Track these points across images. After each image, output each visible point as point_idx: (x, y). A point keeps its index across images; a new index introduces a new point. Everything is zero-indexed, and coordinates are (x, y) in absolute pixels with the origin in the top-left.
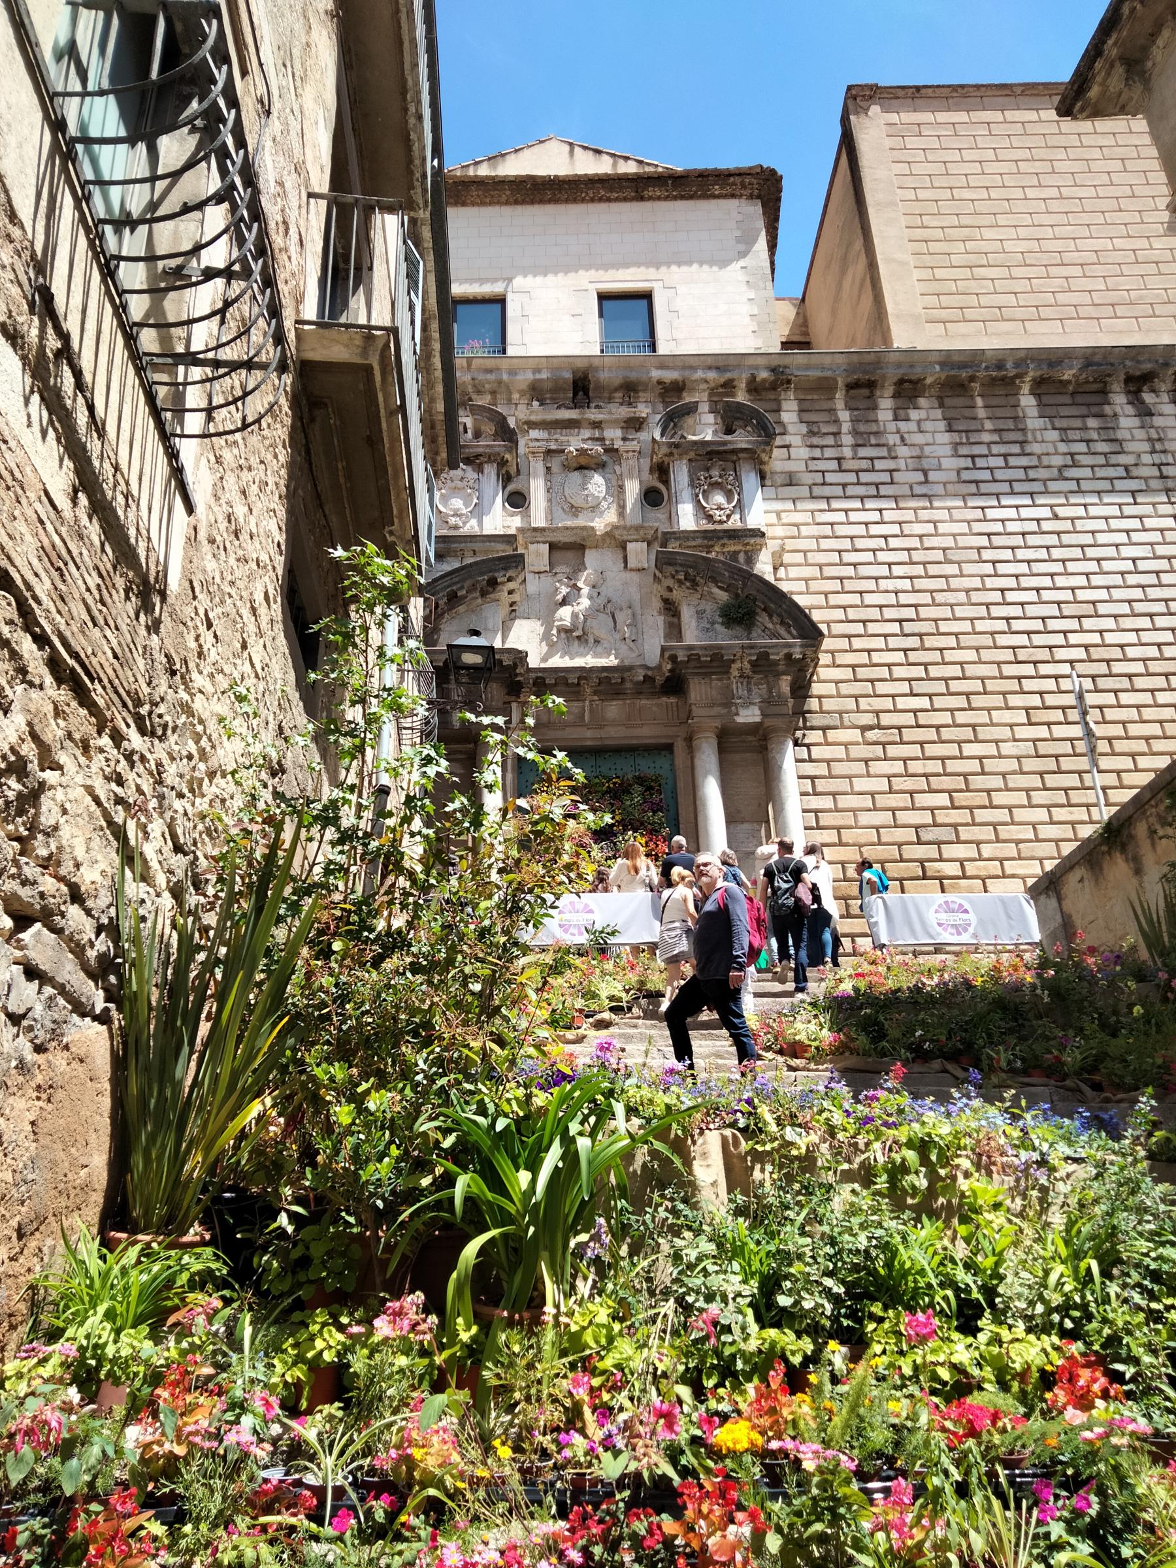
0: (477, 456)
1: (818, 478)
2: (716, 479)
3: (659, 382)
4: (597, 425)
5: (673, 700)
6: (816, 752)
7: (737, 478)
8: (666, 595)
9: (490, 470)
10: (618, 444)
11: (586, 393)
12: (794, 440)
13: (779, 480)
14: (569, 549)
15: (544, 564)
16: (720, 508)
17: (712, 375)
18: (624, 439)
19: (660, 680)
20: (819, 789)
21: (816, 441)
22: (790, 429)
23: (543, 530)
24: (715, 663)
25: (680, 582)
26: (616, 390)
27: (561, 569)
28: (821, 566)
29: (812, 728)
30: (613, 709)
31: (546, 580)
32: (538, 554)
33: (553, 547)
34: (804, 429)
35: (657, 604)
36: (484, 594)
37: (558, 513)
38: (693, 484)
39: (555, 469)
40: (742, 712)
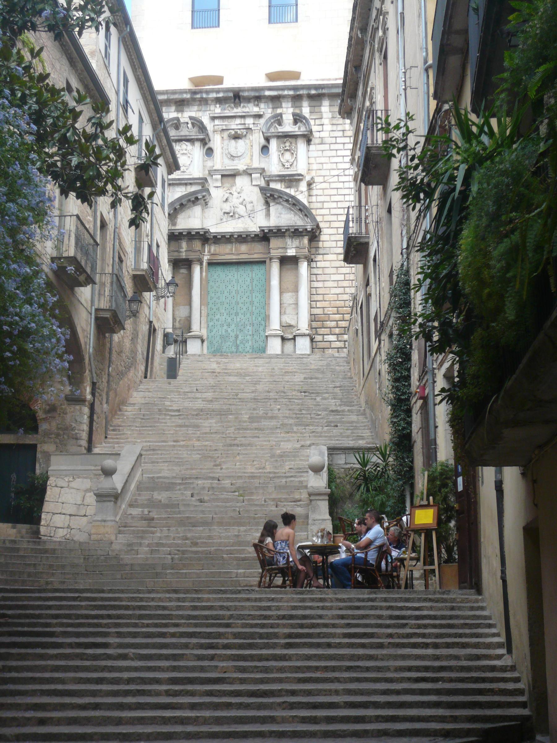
0: (192, 139)
1: (333, 140)
2: (288, 148)
4: (243, 117)
7: (296, 147)
9: (198, 144)
12: (326, 121)
14: (230, 176)
15: (219, 184)
16: (288, 161)
21: (335, 122)
22: (325, 115)
24: (279, 233)
27: (227, 185)
30: (244, 248)
31: (220, 190)
32: (216, 180)
33: (223, 176)
34: (330, 115)
35: (262, 201)
37: (227, 161)
40: (289, 251)
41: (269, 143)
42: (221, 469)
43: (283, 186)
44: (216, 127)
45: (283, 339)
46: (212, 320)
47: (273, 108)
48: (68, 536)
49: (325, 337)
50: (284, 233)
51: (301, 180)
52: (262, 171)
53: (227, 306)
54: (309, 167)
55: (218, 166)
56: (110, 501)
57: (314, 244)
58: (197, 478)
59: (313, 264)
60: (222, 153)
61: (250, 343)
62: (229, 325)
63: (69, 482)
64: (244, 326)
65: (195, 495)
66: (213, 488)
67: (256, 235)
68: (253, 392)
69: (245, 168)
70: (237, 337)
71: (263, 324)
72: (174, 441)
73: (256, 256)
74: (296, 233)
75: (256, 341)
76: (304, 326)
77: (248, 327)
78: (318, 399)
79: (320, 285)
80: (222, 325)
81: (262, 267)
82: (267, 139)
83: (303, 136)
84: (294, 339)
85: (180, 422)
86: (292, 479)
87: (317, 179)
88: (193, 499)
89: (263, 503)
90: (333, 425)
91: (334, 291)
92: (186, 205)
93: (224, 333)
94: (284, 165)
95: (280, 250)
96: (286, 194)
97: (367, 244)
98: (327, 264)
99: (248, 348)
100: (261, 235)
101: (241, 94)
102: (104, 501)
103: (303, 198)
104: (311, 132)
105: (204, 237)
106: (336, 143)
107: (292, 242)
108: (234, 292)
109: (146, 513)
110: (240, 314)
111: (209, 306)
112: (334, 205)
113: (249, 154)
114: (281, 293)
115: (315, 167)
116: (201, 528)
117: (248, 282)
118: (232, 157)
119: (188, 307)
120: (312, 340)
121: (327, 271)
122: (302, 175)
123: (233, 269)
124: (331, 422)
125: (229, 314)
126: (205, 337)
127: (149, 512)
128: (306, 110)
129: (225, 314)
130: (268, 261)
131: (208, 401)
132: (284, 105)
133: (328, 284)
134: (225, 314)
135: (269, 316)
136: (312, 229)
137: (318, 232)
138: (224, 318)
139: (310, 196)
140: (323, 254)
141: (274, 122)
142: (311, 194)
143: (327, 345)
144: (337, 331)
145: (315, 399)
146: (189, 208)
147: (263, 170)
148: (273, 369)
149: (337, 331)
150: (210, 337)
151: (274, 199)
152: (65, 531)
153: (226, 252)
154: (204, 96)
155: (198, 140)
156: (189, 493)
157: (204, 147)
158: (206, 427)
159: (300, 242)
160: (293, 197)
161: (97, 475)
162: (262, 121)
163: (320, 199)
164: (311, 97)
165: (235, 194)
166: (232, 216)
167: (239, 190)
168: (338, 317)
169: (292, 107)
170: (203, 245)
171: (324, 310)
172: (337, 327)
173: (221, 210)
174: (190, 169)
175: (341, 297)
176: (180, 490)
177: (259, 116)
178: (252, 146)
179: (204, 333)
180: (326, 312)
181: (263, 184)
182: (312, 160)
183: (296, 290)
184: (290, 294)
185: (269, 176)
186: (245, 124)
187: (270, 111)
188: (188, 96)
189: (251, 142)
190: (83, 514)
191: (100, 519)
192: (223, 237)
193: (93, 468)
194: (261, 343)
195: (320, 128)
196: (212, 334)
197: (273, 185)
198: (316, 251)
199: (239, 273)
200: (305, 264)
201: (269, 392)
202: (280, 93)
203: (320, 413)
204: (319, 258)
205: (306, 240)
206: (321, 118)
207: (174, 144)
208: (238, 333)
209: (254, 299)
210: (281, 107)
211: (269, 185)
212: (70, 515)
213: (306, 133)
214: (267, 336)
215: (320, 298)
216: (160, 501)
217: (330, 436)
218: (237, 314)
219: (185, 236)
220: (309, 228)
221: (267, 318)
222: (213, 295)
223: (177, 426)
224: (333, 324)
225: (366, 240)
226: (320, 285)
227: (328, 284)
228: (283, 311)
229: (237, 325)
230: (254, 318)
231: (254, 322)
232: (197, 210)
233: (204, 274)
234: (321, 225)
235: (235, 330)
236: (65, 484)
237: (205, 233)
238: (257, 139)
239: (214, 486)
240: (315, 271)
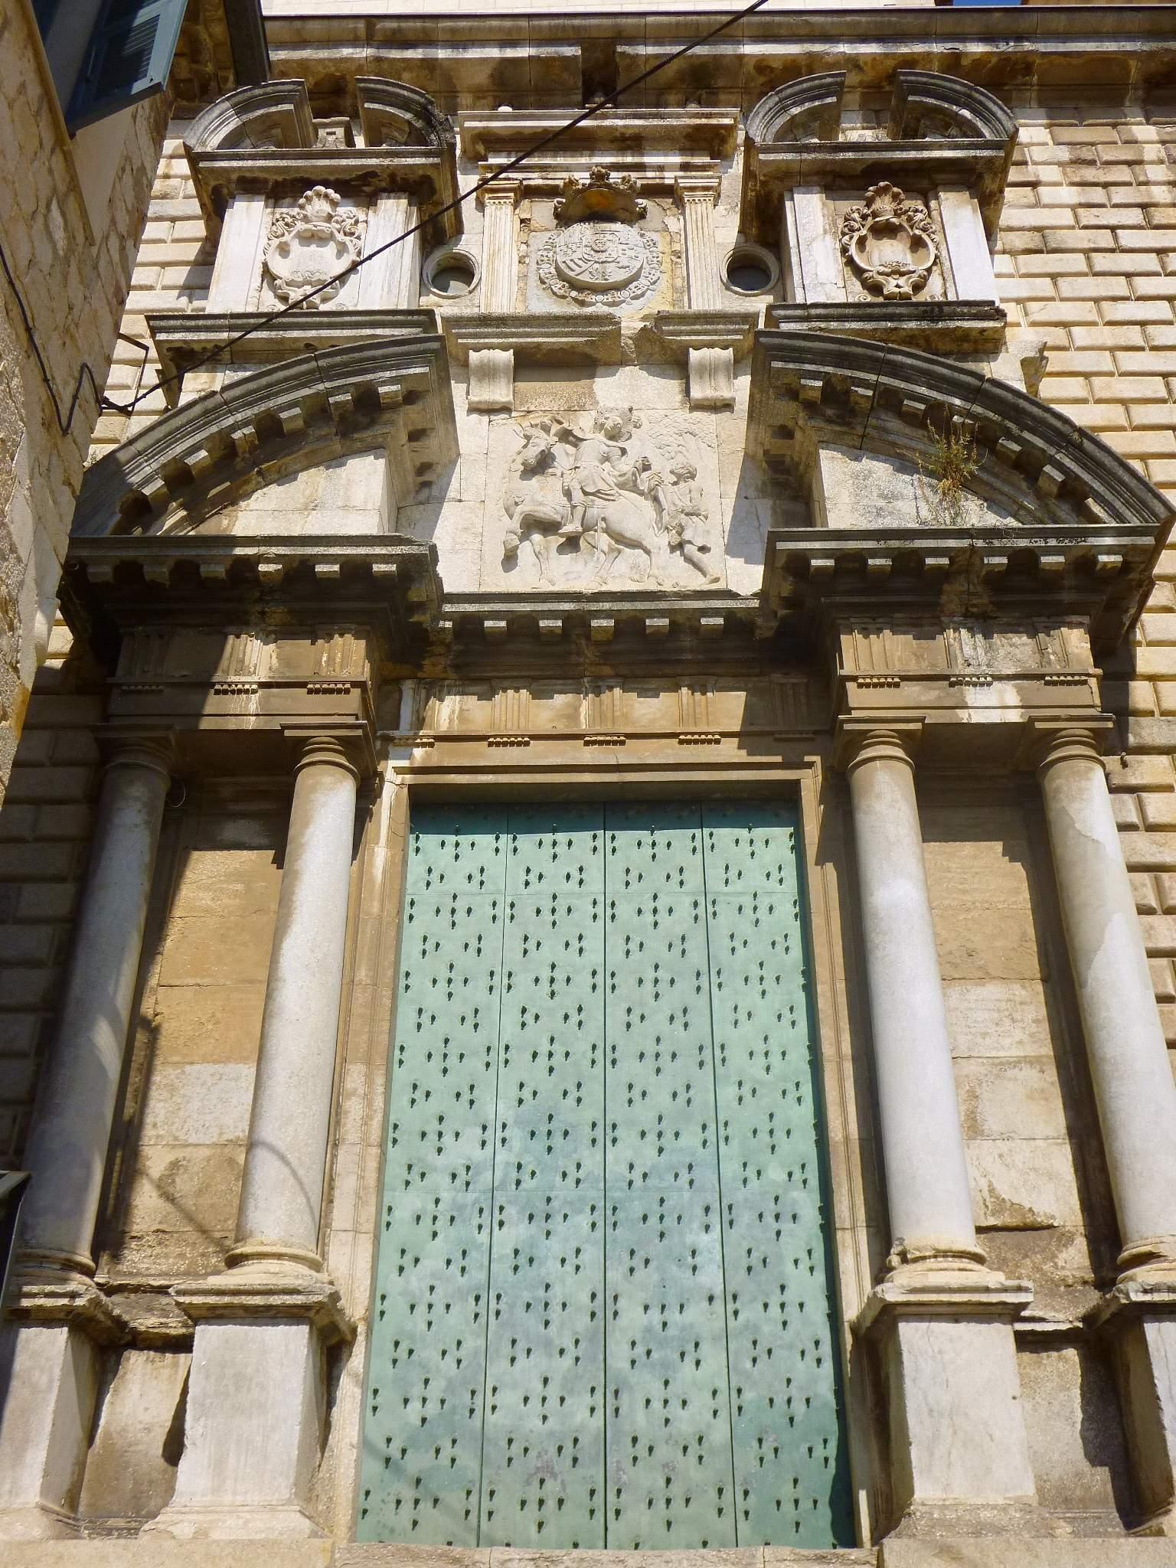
8: (779, 446)
19: (766, 628)
21: (1090, 174)
23: (501, 321)
25: (810, 407)
53: (536, 1074)
61: (713, 1358)
62: (542, 1215)
64: (662, 1220)
67: (738, 624)
70: (605, 1307)
75: (761, 1351)
95: (912, 693)
99: (701, 1403)
108: (584, 980)
111: (402, 1076)
117: (680, 922)
126: (354, 1307)
129: (516, 1135)
150: (396, 1306)
165: (596, 443)
179: (349, 1273)
184: (992, 991)
192: (523, 627)
196: (416, 1280)
199: (617, 864)
218: (606, 1133)
222: (434, 999)
229: (608, 1215)
230: (731, 1169)
231: (737, 1195)
233: (380, 855)
235: (591, 1255)
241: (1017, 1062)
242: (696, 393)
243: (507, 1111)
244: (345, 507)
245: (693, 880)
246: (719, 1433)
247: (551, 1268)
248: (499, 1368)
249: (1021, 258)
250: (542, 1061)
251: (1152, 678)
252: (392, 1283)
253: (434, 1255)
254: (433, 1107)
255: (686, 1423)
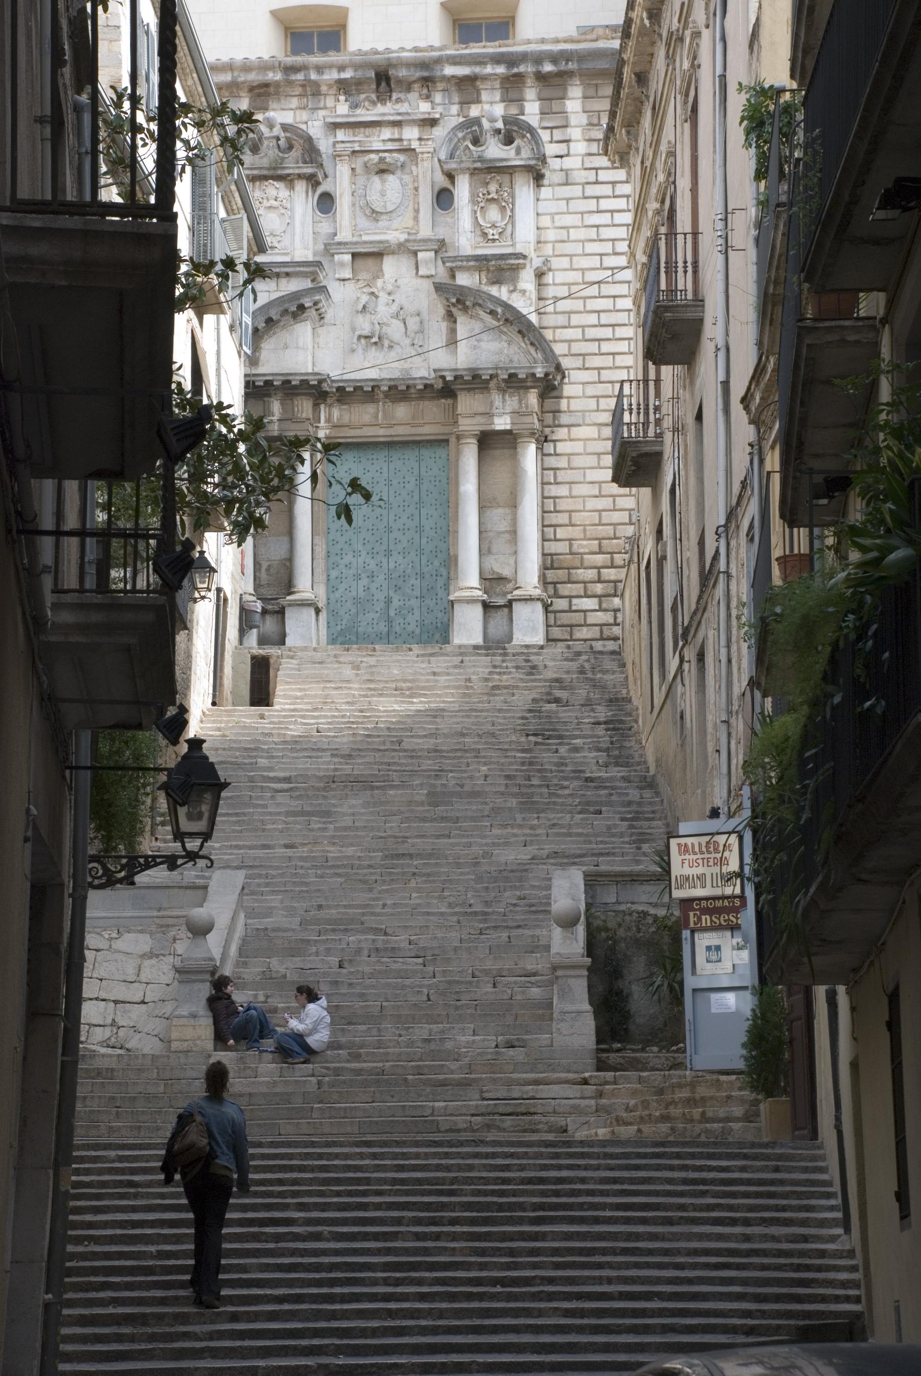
0: (289, 175)
1: (591, 176)
2: (494, 195)
3: (453, 77)
4: (397, 124)
5: (450, 401)
6: (561, 447)
9: (301, 186)
10: (415, 145)
11: (388, 84)
12: (575, 133)
13: (558, 178)
14: (369, 257)
15: (347, 274)
16: (494, 226)
17: (501, 70)
18: (420, 139)
20: (559, 480)
22: (573, 120)
23: (346, 243)
24: (476, 381)
26: (414, 82)
27: (363, 275)
28: (583, 270)
29: (560, 426)
30: (402, 411)
31: (350, 286)
32: (342, 264)
33: (354, 255)
34: (583, 119)
35: (441, 311)
36: (295, 316)
37: (363, 222)
38: (474, 200)
39: (358, 171)
41: (453, 183)
42: (384, 905)
43: (484, 281)
44: (339, 147)
45: (486, 606)
46: (335, 565)
47: (461, 103)
48: (113, 1040)
49: (575, 601)
50: (487, 382)
51: (523, 266)
52: (440, 247)
54: (539, 236)
55: (345, 235)
56: (203, 981)
57: (549, 403)
58: (346, 930)
59: (549, 448)
60: (354, 205)
62: (372, 576)
63: (111, 939)
65: (346, 965)
66: (377, 949)
68: (431, 735)
69: (403, 237)
70: (388, 601)
71: (445, 573)
72: (287, 846)
73: (427, 430)
74: (514, 383)
75: (430, 610)
76: (530, 578)
77: (413, 581)
78: (563, 750)
79: (563, 491)
80: (358, 577)
81: (441, 452)
82: (451, 177)
83: (528, 169)
84: (509, 605)
85: (295, 804)
86: (520, 931)
87: (556, 263)
88: (344, 971)
89: (470, 979)
90: (592, 809)
91: (591, 504)
92: (279, 321)
93: (361, 594)
94: (485, 235)
95: (480, 419)
96: (492, 298)
97: (659, 455)
98: (578, 447)
99: (413, 624)
100: (439, 385)
101: (391, 72)
102: (194, 981)
103: (524, 305)
104: (543, 159)
105: (317, 391)
106: (597, 182)
107: (504, 400)
109: (262, 998)
110: (394, 553)
112: (593, 319)
113: (411, 208)
114: (483, 507)
115: (551, 235)
116: (364, 1027)
118: (375, 215)
119: (286, 539)
120: (547, 608)
121: (577, 462)
122: (525, 257)
123: (382, 455)
124: (588, 803)
125: (372, 553)
127: (267, 997)
128: (532, 111)
129: (364, 553)
130: (453, 440)
131: (342, 756)
132: (485, 96)
133: (579, 490)
134: (364, 553)
135: (456, 558)
136: (547, 375)
137: (559, 378)
138: (361, 560)
139: (540, 299)
140: (569, 426)
141: (464, 138)
142: (544, 295)
143: (577, 618)
144: (599, 588)
145: (557, 751)
146: (284, 327)
147: (442, 243)
148: (469, 680)
149: (599, 588)
151: (465, 309)
152: (108, 1032)
153: (363, 420)
154: (313, 76)
155: (300, 176)
156: (334, 960)
157: (314, 192)
158: (344, 815)
159: (520, 402)
160: (507, 306)
161: (162, 926)
162: (439, 132)
163: (562, 305)
164: (541, 77)
166: (376, 343)
167: (390, 287)
168: (600, 559)
169: (503, 101)
170: (316, 406)
171: (571, 546)
172: (599, 581)
173: (353, 329)
174: (286, 241)
175: (607, 517)
176: (317, 954)
177: (432, 122)
178: (416, 189)
179: (320, 594)
180: (575, 549)
181: (441, 273)
182: (545, 221)
183: (514, 504)
184: (500, 511)
185: (455, 258)
186: (400, 140)
187: (455, 109)
188: (279, 76)
189: (416, 179)
190: (139, 1000)
191: (185, 1013)
193: (155, 913)
194: (440, 615)
195: (560, 149)
196: (338, 594)
197: (463, 280)
198: (554, 418)
199: (392, 466)
200: (532, 447)
201: (463, 735)
202: (477, 70)
203: (566, 783)
204: (562, 433)
205: (533, 398)
206: (566, 126)
207: (249, 186)
208: (391, 593)
209: (424, 521)
210: (478, 101)
211: (453, 277)
212: (116, 1002)
213: (532, 162)
214: (452, 602)
215: (563, 518)
216: (285, 976)
217: (587, 835)
218: (388, 553)
219: (277, 388)
220: (540, 372)
221: (451, 562)
223: (288, 814)
224: (591, 574)
225: (657, 448)
226: (563, 491)
227: (579, 490)
228: (485, 547)
229: (389, 577)
230: (424, 562)
231: (425, 570)
232: (303, 331)
234: (565, 363)
236: (103, 944)
237: (320, 382)
238: (428, 175)
239: (379, 945)
240: (551, 462)
241: (503, 532)
242: (420, 273)
243: (360, 547)
244: (297, 347)
245: (416, 472)
246: (418, 631)
247: (373, 590)
248: (361, 615)
249: (557, 188)
250: (370, 532)
251: (568, 398)
252: (332, 596)
253: (342, 587)
254: (339, 546)
255: (410, 628)
